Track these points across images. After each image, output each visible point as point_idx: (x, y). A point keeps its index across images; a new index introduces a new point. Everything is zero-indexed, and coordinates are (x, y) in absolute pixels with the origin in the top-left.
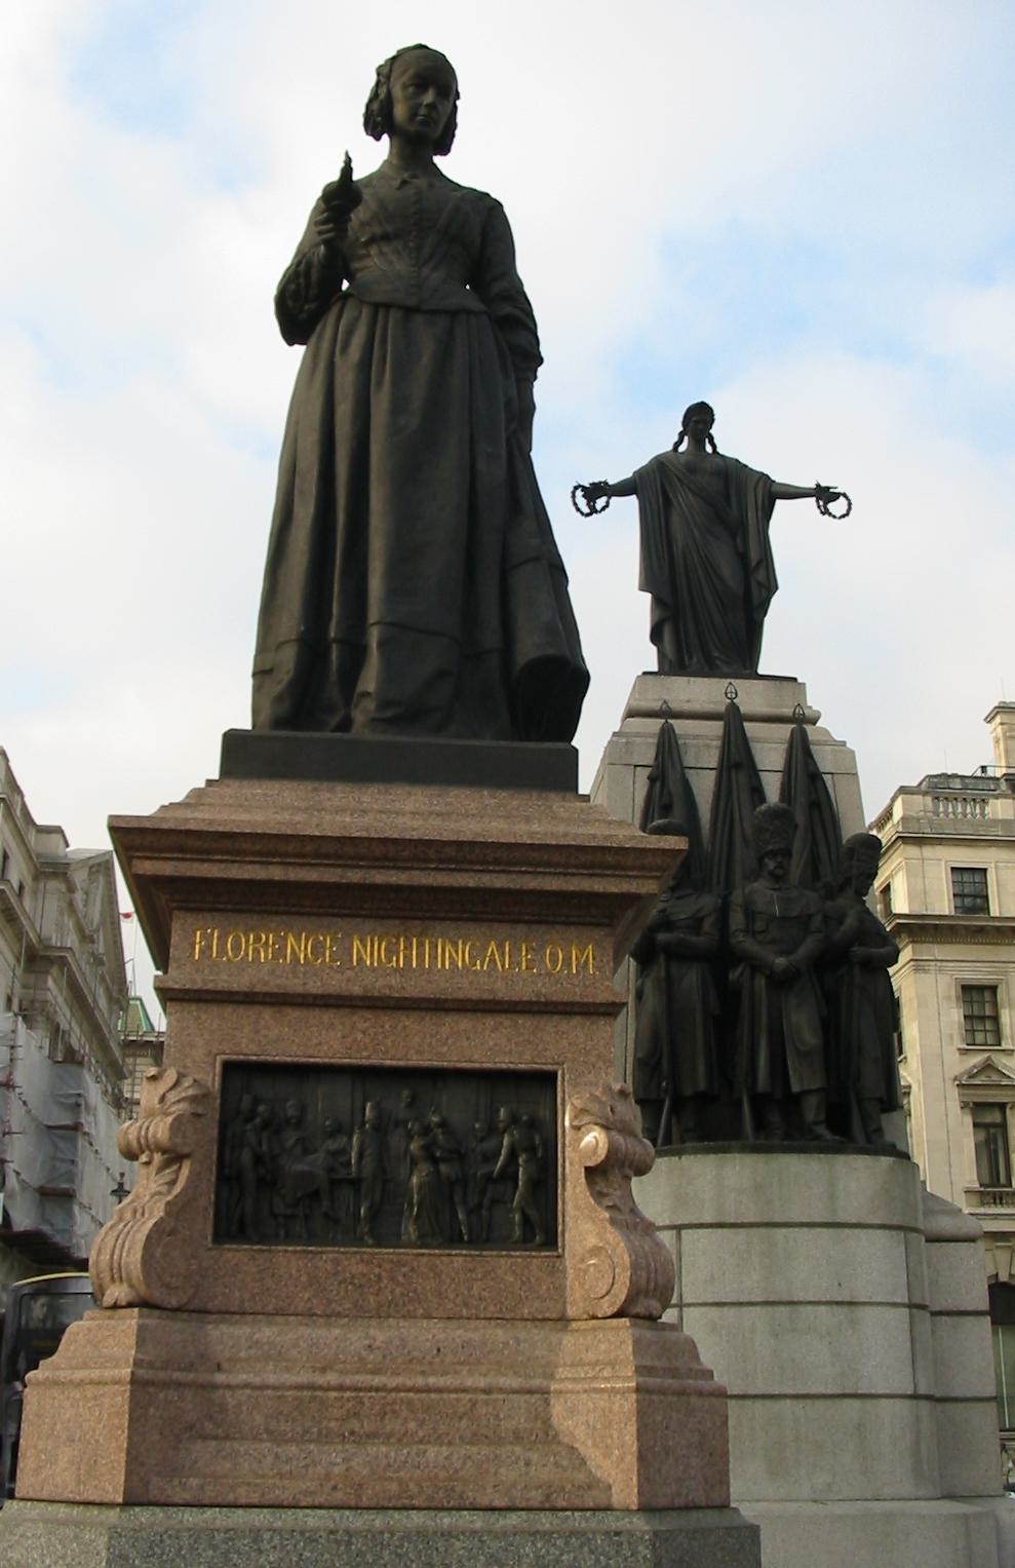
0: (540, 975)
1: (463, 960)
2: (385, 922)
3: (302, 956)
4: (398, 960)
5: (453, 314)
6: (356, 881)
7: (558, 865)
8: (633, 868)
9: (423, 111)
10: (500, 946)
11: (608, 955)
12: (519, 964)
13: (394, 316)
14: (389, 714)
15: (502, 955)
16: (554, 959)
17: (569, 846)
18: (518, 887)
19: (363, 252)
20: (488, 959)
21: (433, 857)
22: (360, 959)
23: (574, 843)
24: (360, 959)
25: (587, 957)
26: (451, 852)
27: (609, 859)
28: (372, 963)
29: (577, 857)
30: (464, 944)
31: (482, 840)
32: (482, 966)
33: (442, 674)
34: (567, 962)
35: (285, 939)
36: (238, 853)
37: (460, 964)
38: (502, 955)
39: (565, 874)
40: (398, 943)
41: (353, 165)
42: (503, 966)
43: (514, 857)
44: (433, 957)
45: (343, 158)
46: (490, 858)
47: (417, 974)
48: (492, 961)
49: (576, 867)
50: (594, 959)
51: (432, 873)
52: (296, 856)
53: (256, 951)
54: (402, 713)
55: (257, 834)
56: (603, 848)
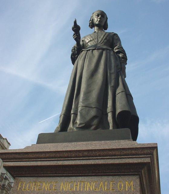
0: (116, 191)
1: (93, 188)
2: (71, 178)
3: (46, 189)
4: (73, 189)
5: (103, 49)
6: (60, 164)
7: (118, 155)
8: (141, 155)
9: (99, 19)
10: (104, 183)
11: (138, 184)
12: (110, 188)
13: (91, 51)
14: (81, 126)
15: (105, 186)
16: (120, 187)
17: (120, 149)
18: (107, 163)
19: (87, 45)
20: (100, 188)
21: (81, 155)
22: (63, 189)
23: (121, 148)
24: (63, 189)
25: (131, 185)
26: (86, 153)
27: (134, 152)
28: (66, 190)
29: (123, 152)
30: (93, 183)
31: (94, 149)
32: (98, 190)
33: (95, 117)
34: (125, 186)
35: (43, 184)
36: (29, 158)
37: (91, 189)
38: (105, 186)
39: (121, 158)
40: (74, 184)
41: (77, 21)
42: (105, 189)
43: (105, 154)
44: (84, 188)
45: (75, 20)
46: (98, 154)
47: (79, 193)
48: (101, 188)
49: (124, 155)
50: (133, 186)
51: (82, 161)
52: (44, 158)
53: (34, 187)
54: (86, 126)
55: (33, 152)
56: (131, 149)
